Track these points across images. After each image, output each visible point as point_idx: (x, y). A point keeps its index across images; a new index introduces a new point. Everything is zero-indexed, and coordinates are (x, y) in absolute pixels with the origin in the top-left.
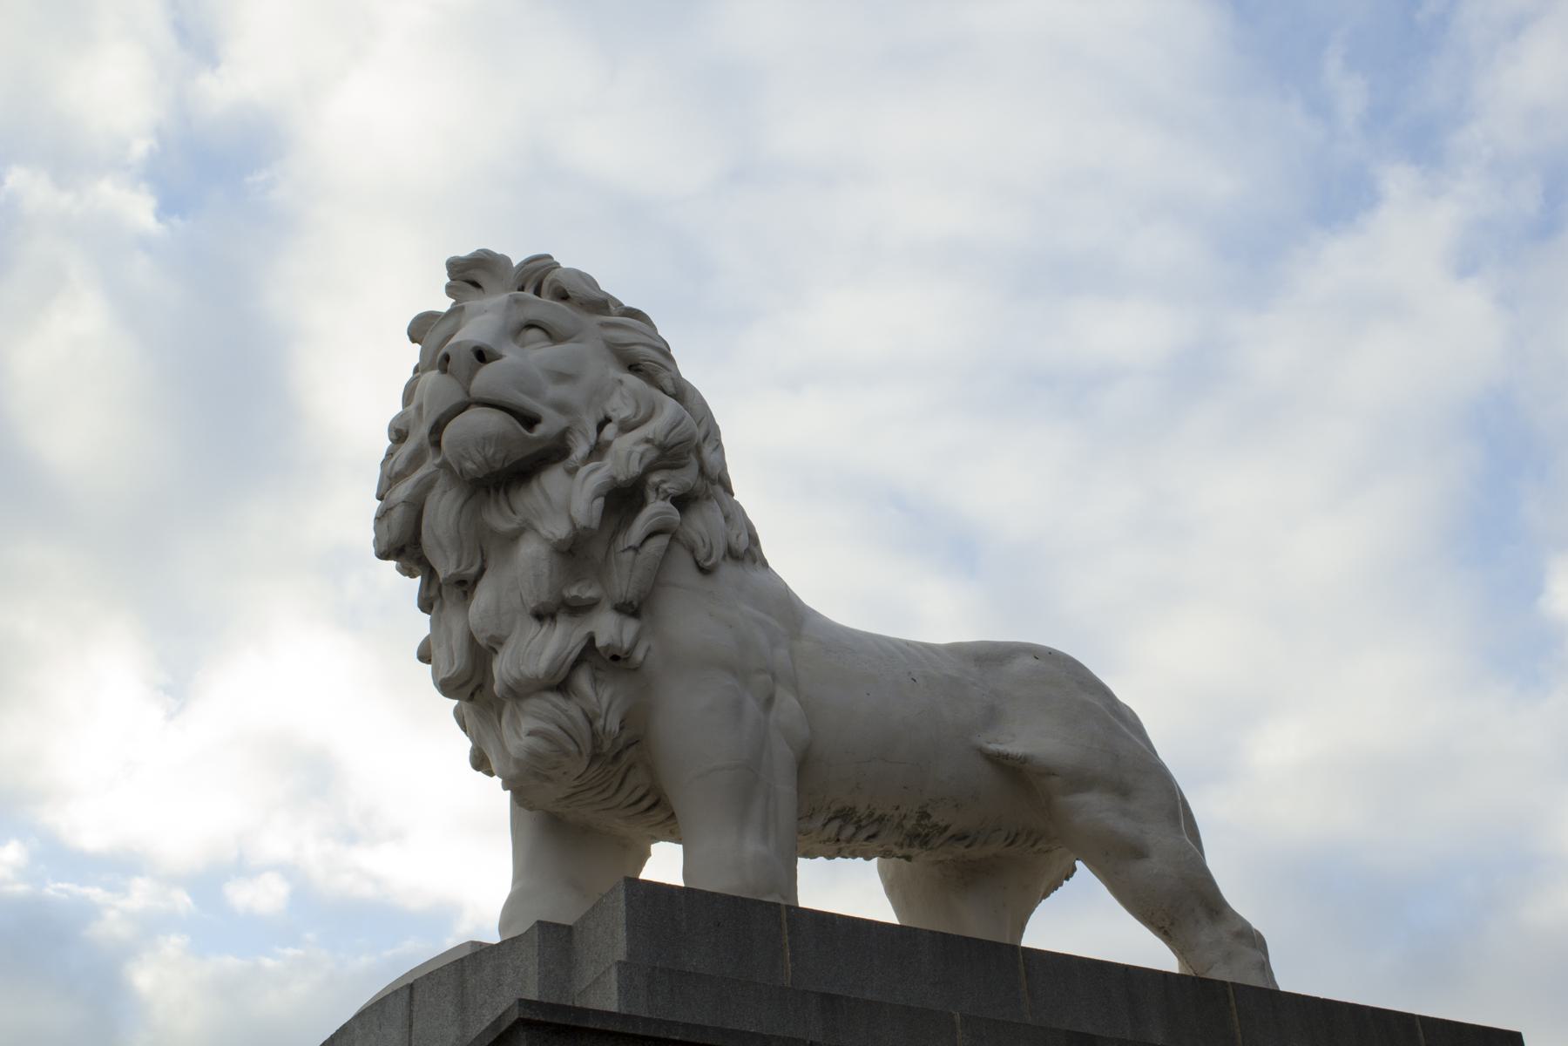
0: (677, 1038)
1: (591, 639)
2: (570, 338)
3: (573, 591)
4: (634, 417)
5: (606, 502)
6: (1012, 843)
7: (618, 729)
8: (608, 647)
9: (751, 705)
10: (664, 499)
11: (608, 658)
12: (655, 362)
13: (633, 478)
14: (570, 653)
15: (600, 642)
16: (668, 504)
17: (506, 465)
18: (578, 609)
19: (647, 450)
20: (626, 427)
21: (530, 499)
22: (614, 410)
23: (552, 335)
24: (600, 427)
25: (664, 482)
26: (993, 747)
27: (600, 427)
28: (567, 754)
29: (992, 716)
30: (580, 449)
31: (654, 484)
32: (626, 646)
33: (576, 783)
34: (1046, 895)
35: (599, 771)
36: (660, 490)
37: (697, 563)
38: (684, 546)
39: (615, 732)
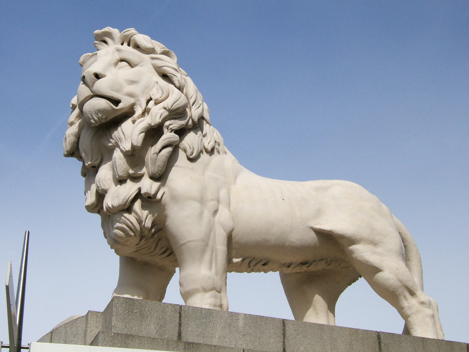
1: (140, 189)
2: (137, 65)
3: (131, 171)
4: (161, 98)
5: (146, 135)
6: (329, 265)
7: (150, 226)
9: (207, 214)
10: (171, 132)
11: (146, 197)
12: (171, 74)
13: (157, 124)
14: (130, 196)
15: (143, 192)
16: (173, 134)
18: (136, 178)
19: (164, 112)
20: (156, 104)
21: (117, 133)
22: (153, 95)
23: (131, 65)
24: (148, 102)
25: (170, 125)
26: (318, 227)
27: (148, 102)
28: (131, 236)
29: (319, 213)
30: (139, 111)
31: (167, 126)
32: (153, 192)
33: (137, 247)
34: (350, 284)
36: (169, 128)
37: (187, 156)
38: (182, 149)
39: (149, 227)
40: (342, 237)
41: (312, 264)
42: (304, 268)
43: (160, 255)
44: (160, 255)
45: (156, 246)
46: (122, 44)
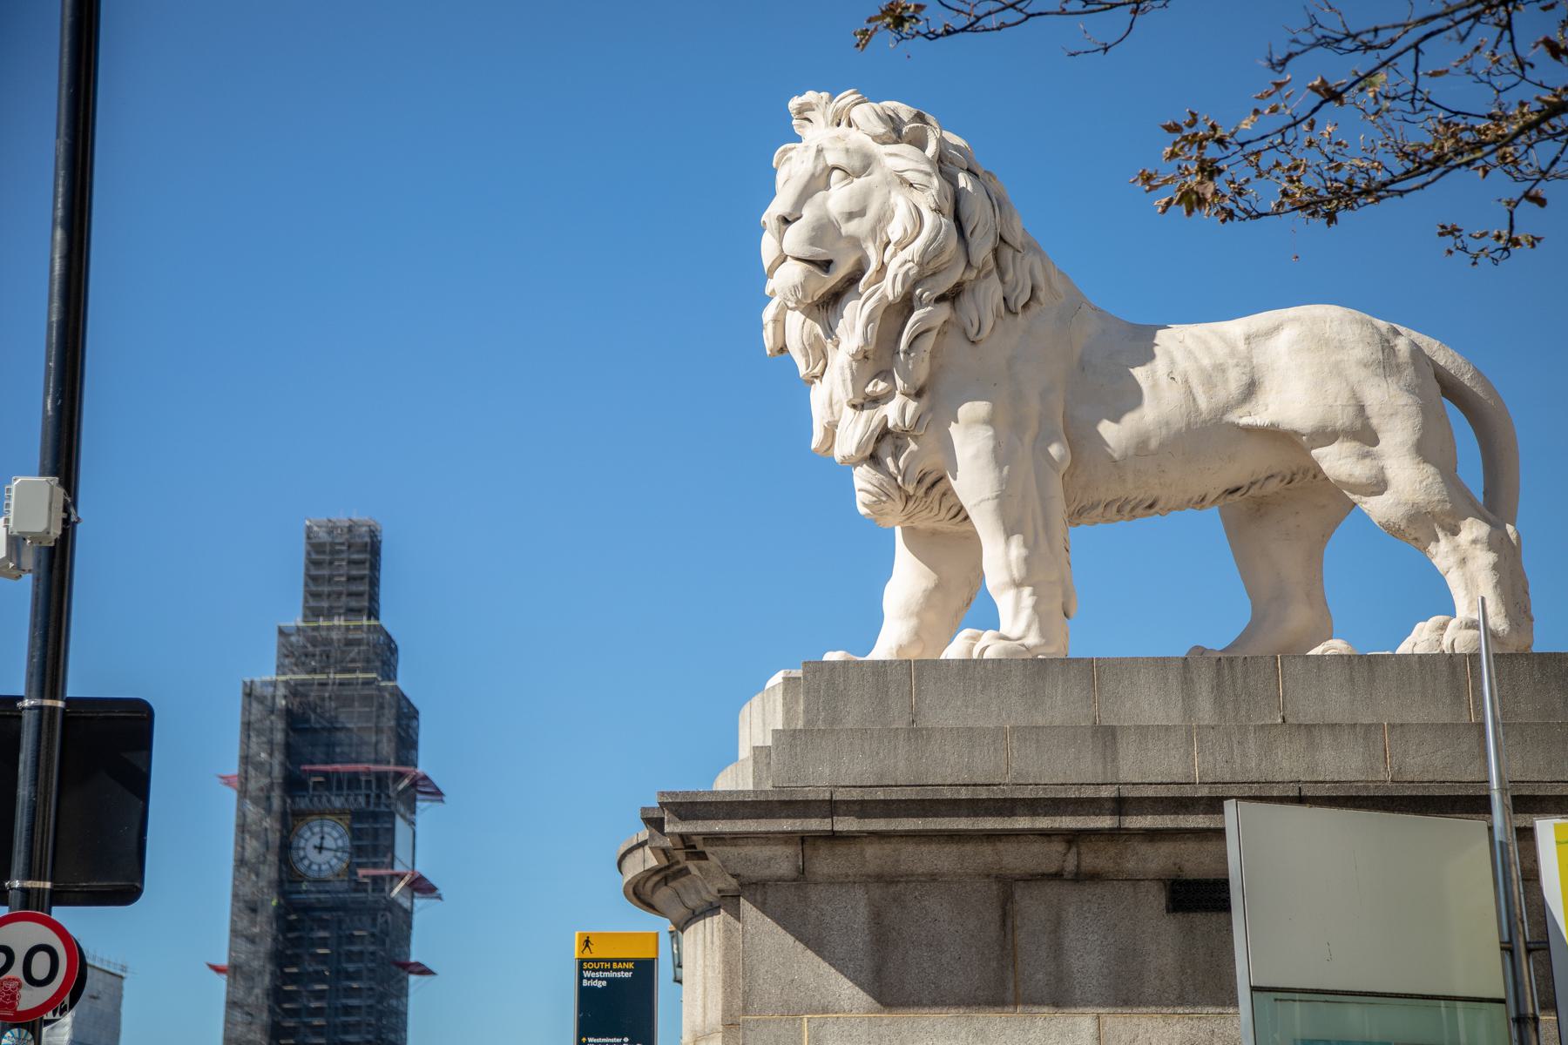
0: (750, 799)
6: (1289, 483)
8: (896, 425)
17: (815, 299)
35: (916, 505)
40: (1296, 432)
41: (1249, 488)
42: (1236, 496)
43: (950, 519)
44: (950, 519)
45: (940, 505)
46: (838, 125)
